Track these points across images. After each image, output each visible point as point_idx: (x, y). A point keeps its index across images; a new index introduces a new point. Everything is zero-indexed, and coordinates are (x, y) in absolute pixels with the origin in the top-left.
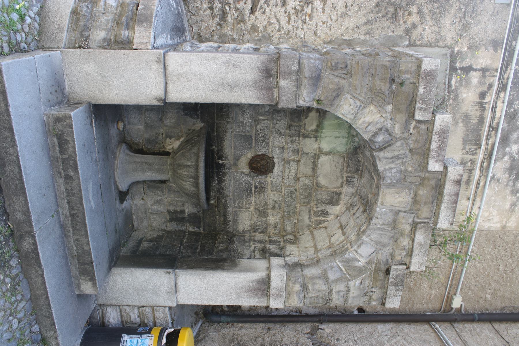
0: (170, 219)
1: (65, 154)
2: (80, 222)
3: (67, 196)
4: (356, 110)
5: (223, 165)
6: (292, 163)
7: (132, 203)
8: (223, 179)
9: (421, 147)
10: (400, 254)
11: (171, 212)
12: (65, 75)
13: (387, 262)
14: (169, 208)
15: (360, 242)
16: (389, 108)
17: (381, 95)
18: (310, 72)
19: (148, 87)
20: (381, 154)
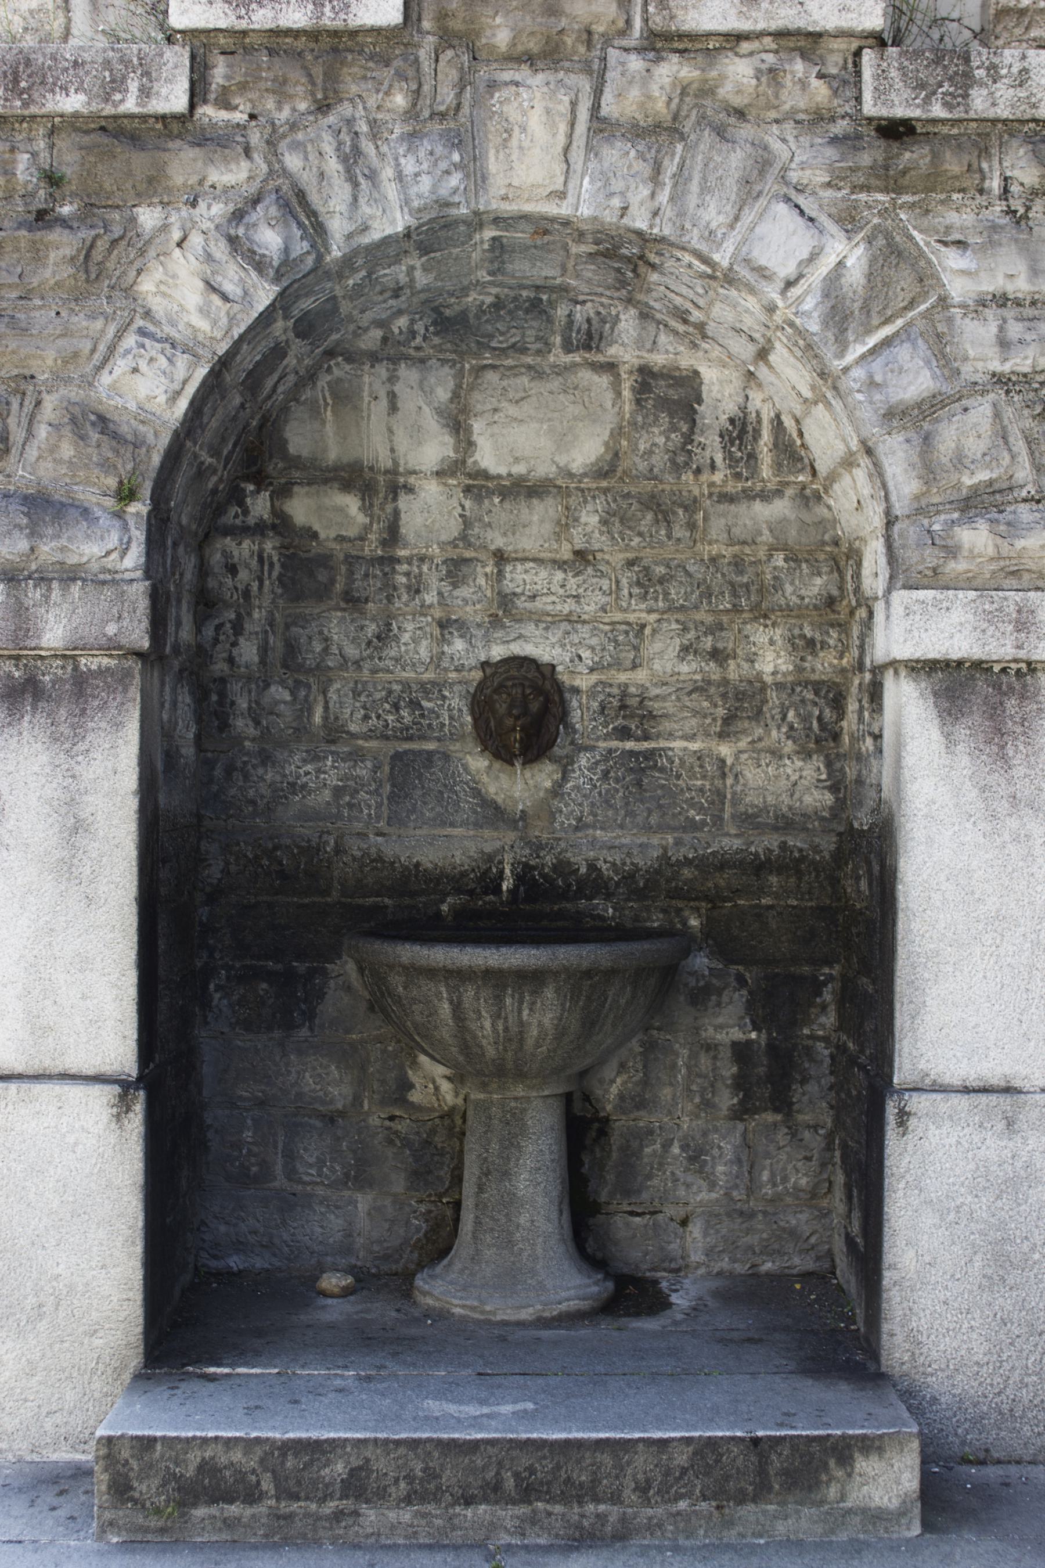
0: (776, 1110)
1: (258, 1483)
2: (558, 1467)
3: (437, 1501)
4: (153, 348)
5: (524, 874)
6: (508, 586)
7: (702, 1271)
8: (588, 874)
9: (304, 68)
10: (804, 84)
11: (741, 1102)
12: (36, 1458)
13: (846, 137)
14: (725, 1112)
15: (744, 272)
16: (148, 217)
17: (97, 255)
18: (9, 532)
19: (76, 1144)
20: (338, 227)
